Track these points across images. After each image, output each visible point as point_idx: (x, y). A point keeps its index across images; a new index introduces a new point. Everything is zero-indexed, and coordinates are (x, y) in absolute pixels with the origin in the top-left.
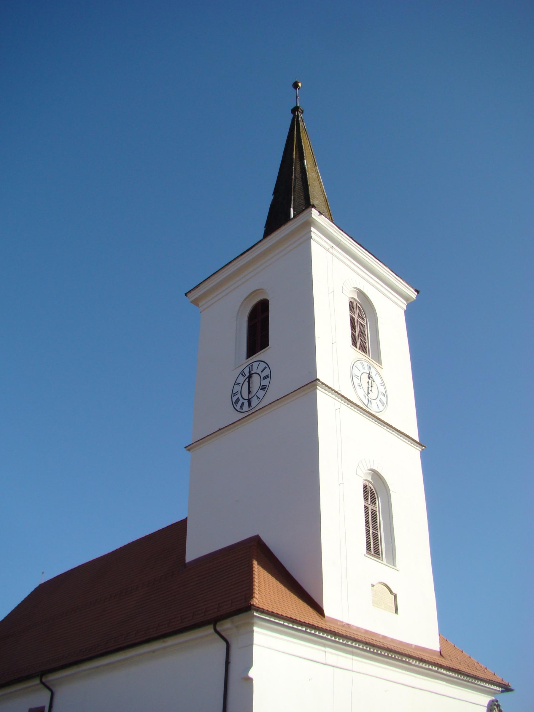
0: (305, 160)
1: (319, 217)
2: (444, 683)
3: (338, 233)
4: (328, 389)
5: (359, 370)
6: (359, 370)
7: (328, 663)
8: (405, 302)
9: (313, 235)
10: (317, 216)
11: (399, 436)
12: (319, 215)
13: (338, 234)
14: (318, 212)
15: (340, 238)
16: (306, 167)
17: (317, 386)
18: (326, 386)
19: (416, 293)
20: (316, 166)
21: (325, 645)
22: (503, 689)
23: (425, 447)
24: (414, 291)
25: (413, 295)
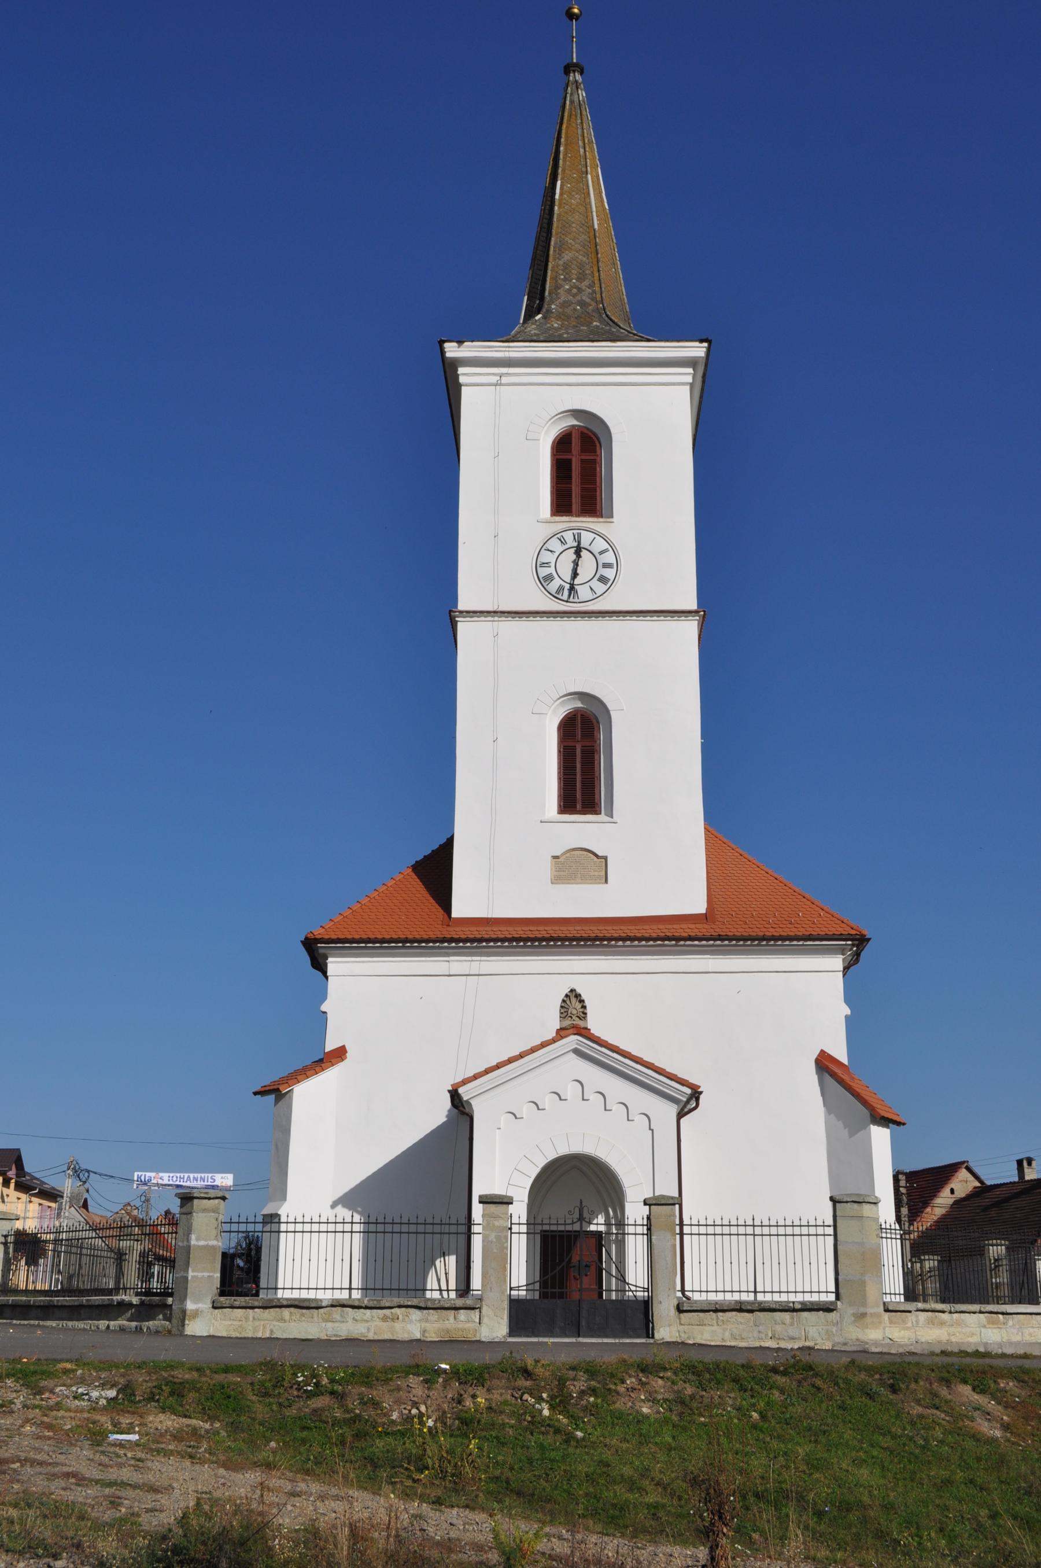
0: (559, 183)
1: (460, 349)
2: (709, 956)
3: (507, 349)
4: (475, 615)
5: (551, 551)
6: (551, 551)
7: (451, 973)
8: (691, 370)
9: (462, 380)
10: (457, 349)
11: (641, 618)
12: (459, 347)
13: (505, 351)
14: (455, 344)
15: (507, 354)
16: (557, 196)
17: (457, 619)
18: (468, 612)
19: (706, 344)
20: (587, 174)
21: (448, 955)
22: (856, 942)
23: (704, 611)
24: (697, 344)
25: (697, 350)
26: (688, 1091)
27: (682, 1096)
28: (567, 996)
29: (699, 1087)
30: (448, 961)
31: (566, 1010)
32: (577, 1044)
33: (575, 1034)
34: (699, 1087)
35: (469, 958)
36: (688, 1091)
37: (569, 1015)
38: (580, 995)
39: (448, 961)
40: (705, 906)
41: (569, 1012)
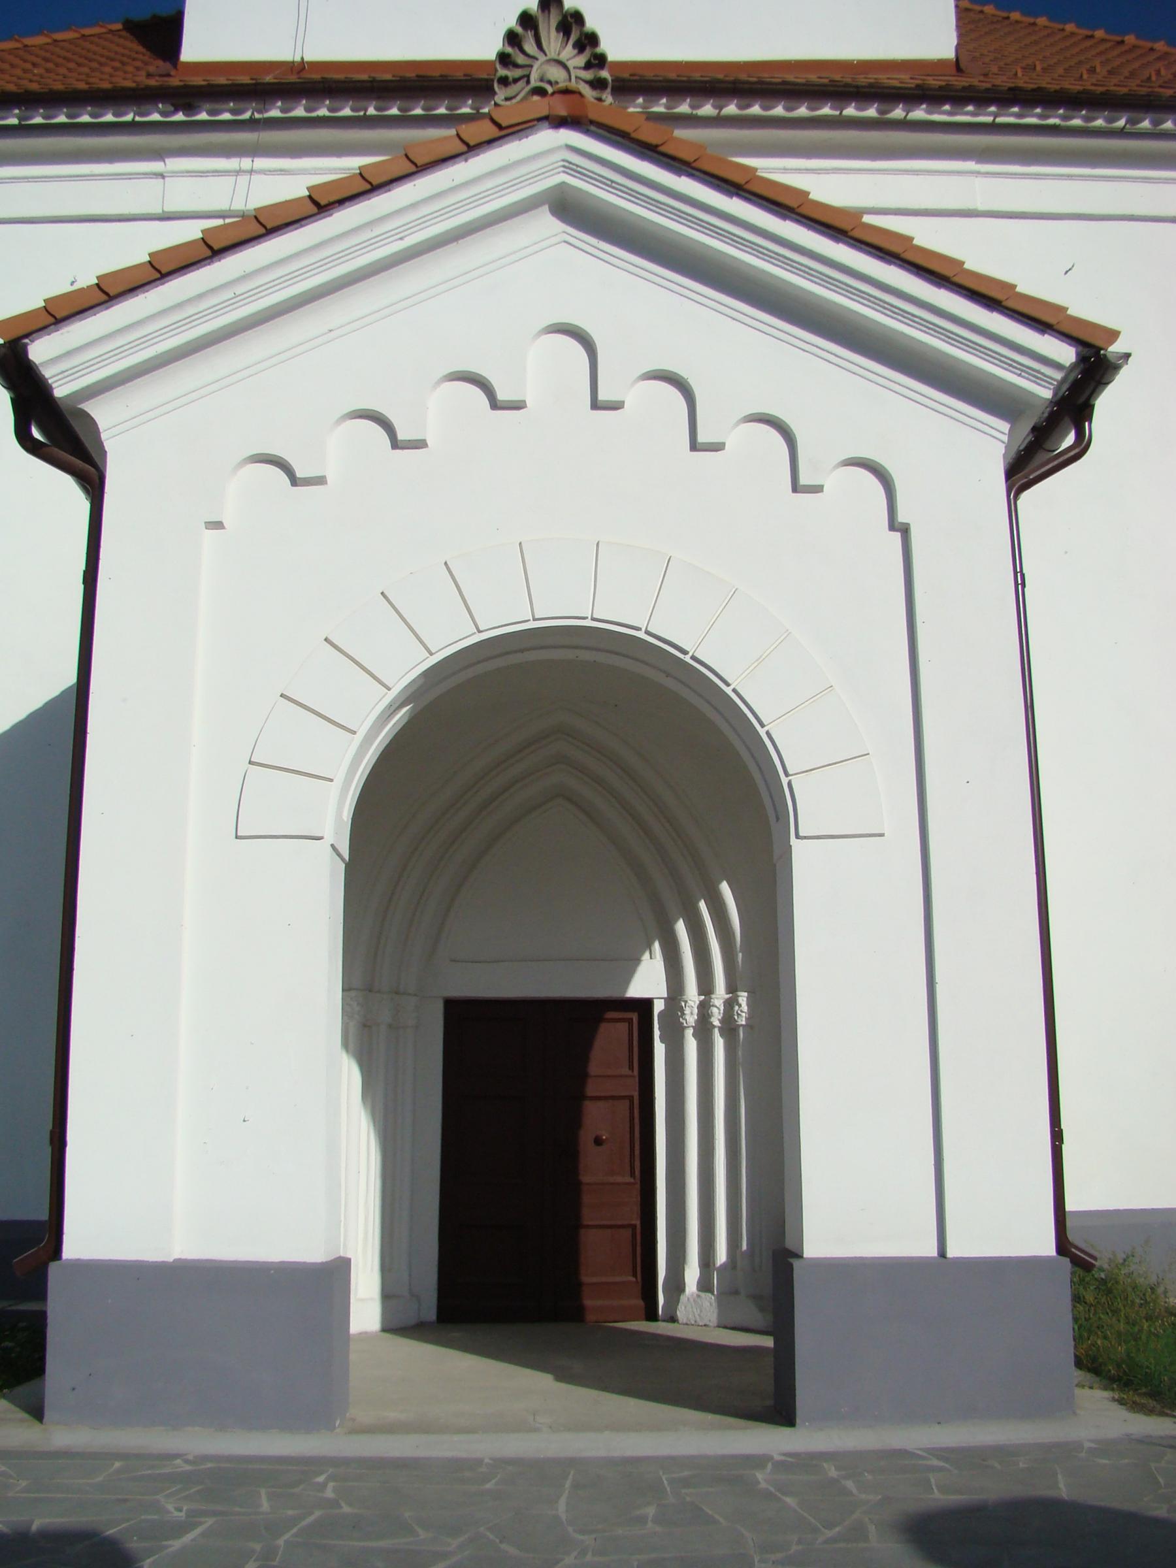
2: (971, 165)
21: (159, 154)
26: (1066, 354)
27: (1037, 377)
28: (526, 19)
29: (1113, 335)
30: (162, 176)
31: (518, 73)
32: (570, 168)
33: (560, 122)
34: (1113, 335)
35: (232, 163)
36: (1066, 354)
37: (534, 82)
38: (578, 17)
39: (162, 176)
40: (954, 41)
41: (534, 76)
